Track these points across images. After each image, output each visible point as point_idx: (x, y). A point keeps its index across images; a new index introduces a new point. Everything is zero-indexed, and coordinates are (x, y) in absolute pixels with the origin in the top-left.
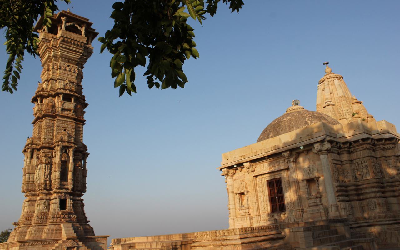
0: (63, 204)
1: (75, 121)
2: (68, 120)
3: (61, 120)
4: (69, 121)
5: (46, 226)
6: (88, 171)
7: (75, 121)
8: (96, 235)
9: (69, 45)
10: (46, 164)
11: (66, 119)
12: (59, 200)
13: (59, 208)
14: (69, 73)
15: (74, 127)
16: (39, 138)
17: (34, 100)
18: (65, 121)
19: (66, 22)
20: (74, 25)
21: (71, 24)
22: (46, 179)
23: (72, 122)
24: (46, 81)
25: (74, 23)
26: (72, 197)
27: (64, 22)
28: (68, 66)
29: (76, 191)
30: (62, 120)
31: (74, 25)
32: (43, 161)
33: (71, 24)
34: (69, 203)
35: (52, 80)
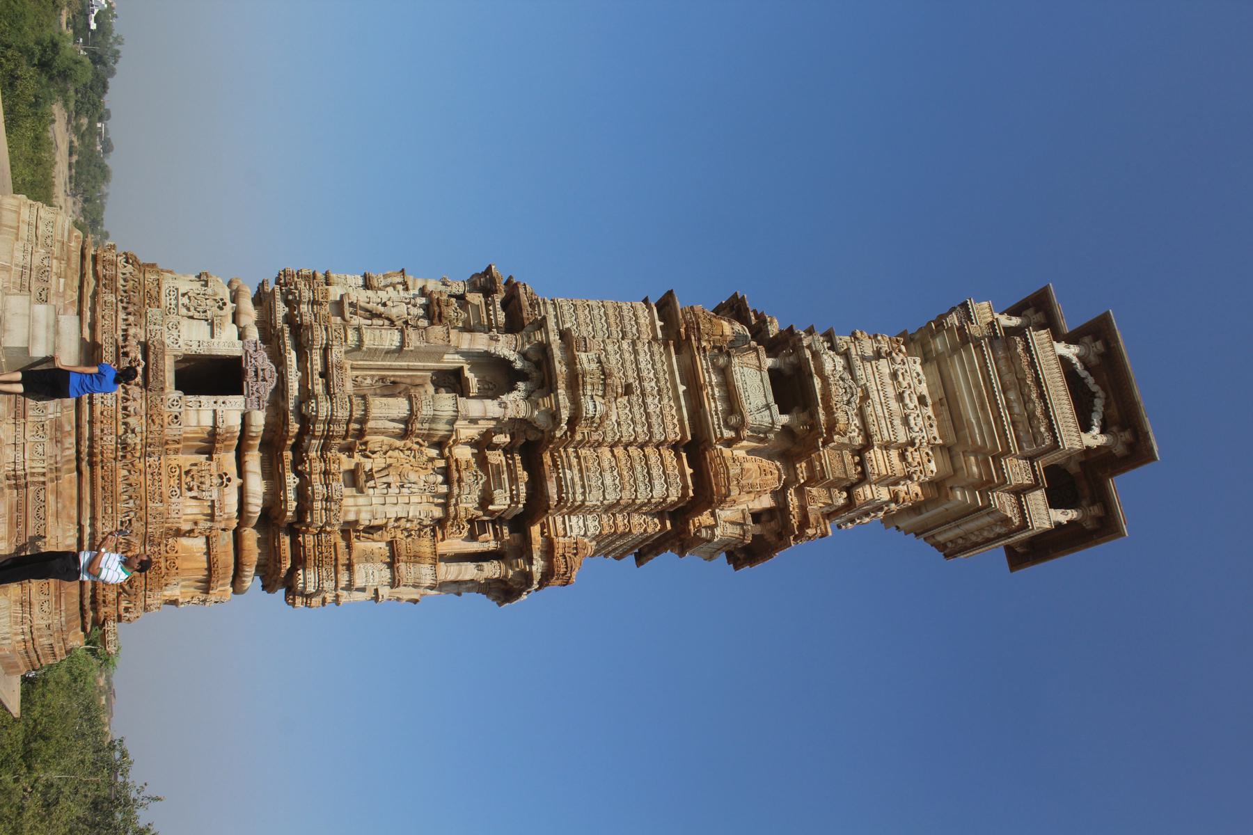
0: (211, 376)
2: (683, 403)
3: (670, 365)
4: (679, 409)
7: (692, 436)
9: (1007, 378)
11: (682, 388)
12: (237, 350)
13: (183, 350)
14: (894, 405)
15: (658, 437)
18: (675, 388)
20: (1093, 395)
22: (347, 311)
23: (681, 421)
25: (1101, 394)
26: (259, 419)
28: (922, 400)
29: (299, 474)
30: (672, 373)
31: (1093, 395)
34: (231, 410)
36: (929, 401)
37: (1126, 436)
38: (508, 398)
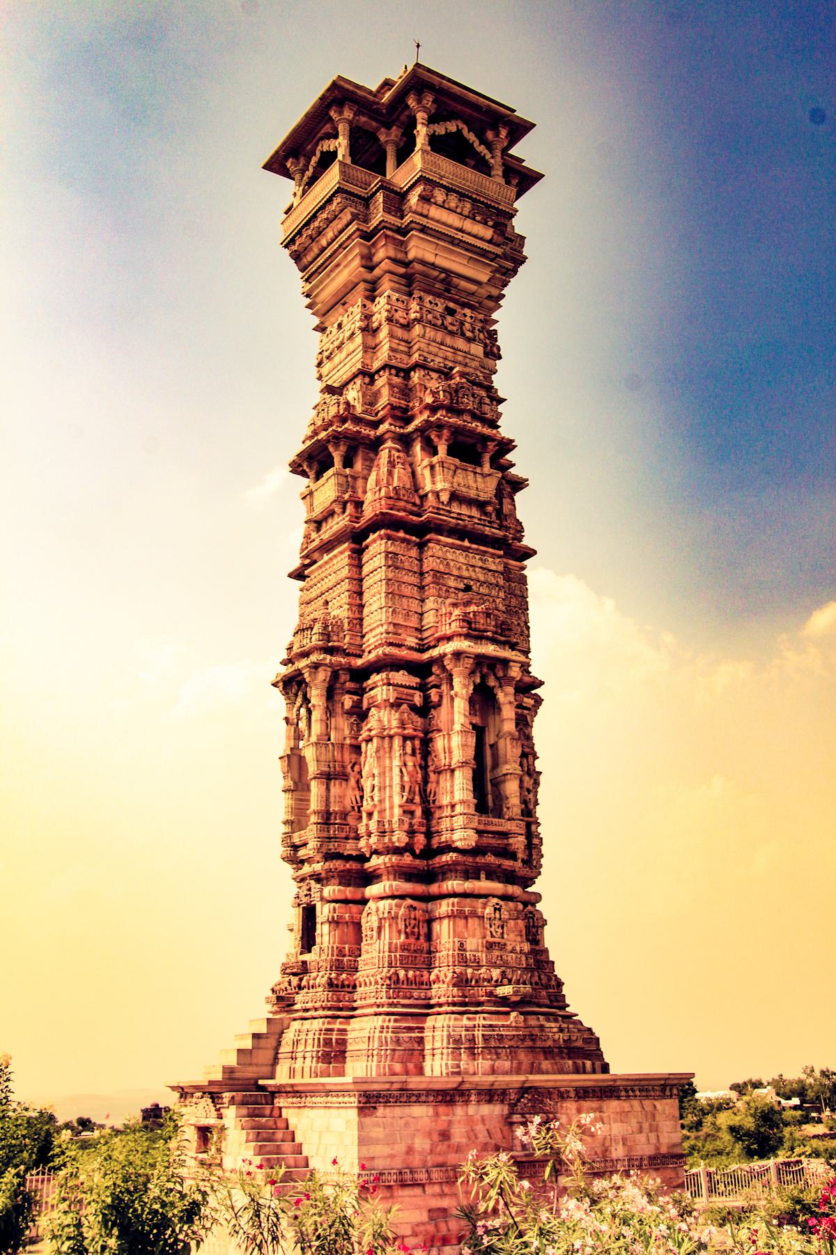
1: (501, 553)
5: (428, 1015)
6: (542, 778)
8: (614, 1070)
10: (405, 738)
16: (358, 621)
17: (313, 461)
19: (431, 120)
20: (459, 131)
21: (452, 127)
24: (362, 373)
25: (461, 125)
27: (421, 116)
31: (459, 131)
32: (389, 721)
33: (452, 127)
35: (391, 367)
36: (451, 305)
37: (503, 133)
38: (501, 696)
